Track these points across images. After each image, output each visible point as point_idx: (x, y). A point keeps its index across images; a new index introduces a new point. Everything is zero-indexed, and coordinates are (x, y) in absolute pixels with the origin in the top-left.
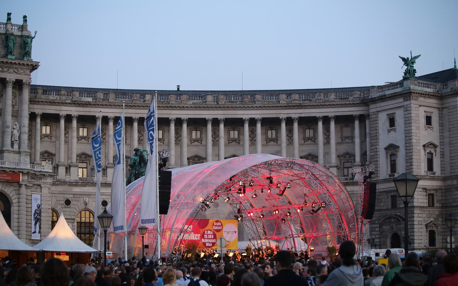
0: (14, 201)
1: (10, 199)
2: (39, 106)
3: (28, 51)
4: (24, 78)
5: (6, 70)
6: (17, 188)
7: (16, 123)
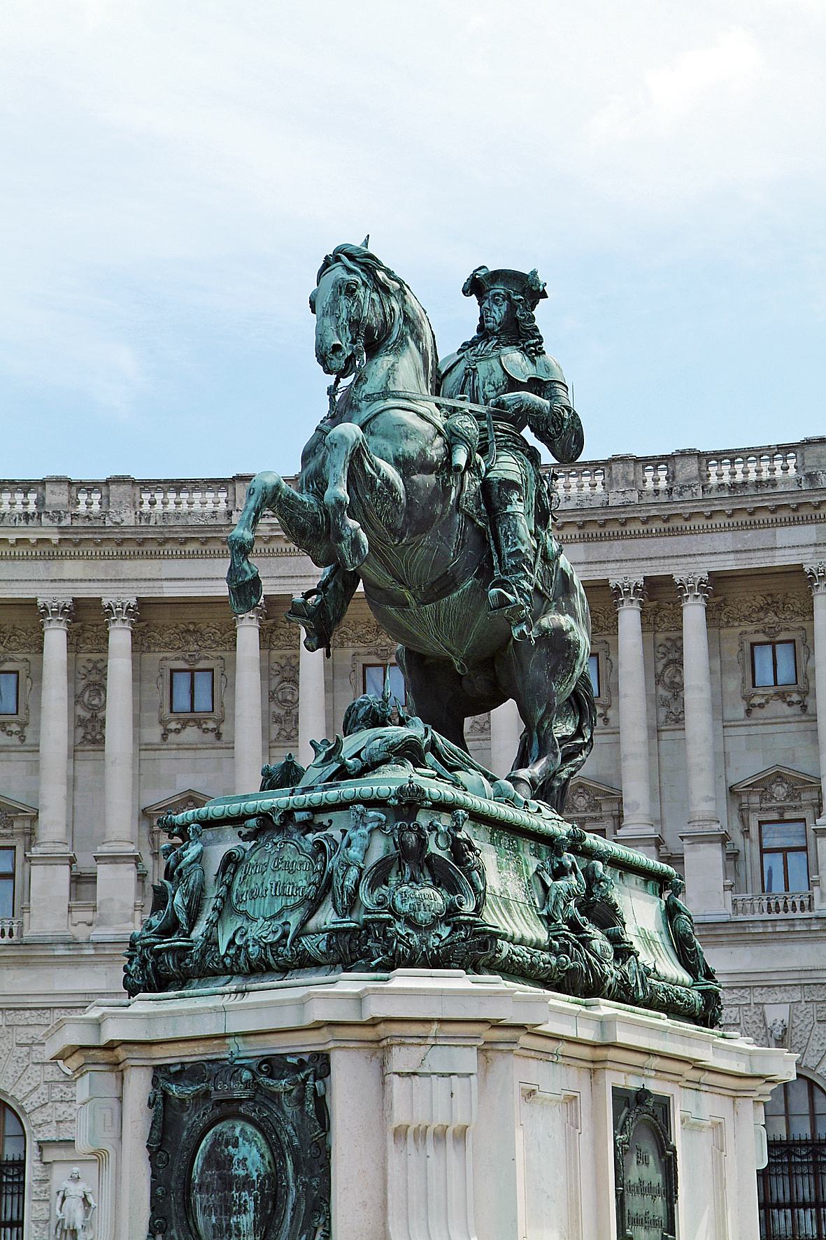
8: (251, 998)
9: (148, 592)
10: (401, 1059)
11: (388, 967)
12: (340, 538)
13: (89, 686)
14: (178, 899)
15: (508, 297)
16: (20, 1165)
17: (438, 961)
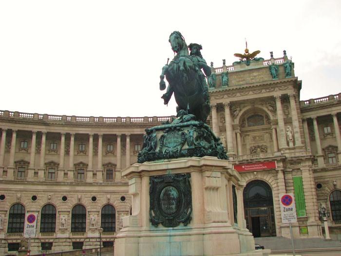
0: (273, 185)
1: (269, 184)
2: (313, 113)
3: (288, 73)
4: (290, 92)
5: (273, 89)
6: (275, 175)
7: (289, 126)
8: (171, 162)
9: (77, 132)
10: (207, 173)
11: (202, 156)
12: (183, 76)
13: (68, 145)
14: (152, 144)
15: (196, 48)
16: (55, 215)
17: (211, 155)
